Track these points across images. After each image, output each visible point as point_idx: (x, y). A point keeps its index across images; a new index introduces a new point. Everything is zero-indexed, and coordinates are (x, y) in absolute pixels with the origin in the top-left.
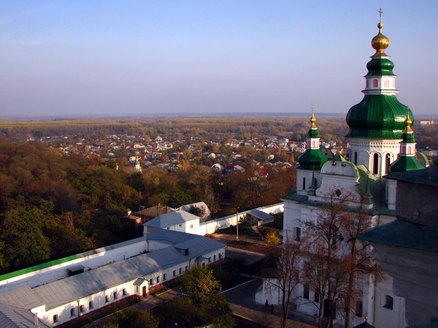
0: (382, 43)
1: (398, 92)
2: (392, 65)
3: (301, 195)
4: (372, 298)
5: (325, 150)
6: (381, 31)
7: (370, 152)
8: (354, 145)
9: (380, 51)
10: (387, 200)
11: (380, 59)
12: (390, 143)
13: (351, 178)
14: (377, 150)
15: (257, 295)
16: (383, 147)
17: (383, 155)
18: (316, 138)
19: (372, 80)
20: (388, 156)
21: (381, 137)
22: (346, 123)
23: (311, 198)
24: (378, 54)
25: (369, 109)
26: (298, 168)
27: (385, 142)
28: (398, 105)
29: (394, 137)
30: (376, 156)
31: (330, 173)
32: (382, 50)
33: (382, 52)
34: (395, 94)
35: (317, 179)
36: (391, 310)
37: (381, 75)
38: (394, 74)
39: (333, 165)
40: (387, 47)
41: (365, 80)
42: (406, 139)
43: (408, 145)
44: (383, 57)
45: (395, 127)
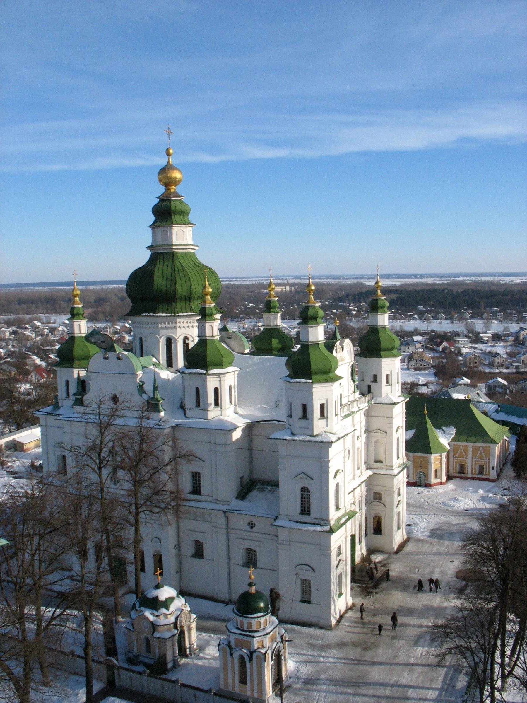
0: (172, 177)
6: (170, 160)
9: (170, 189)
14: (170, 333)
16: (178, 329)
17: (179, 340)
19: (159, 231)
30: (169, 342)
32: (173, 187)
33: (172, 190)
36: (201, 560)
39: (105, 358)
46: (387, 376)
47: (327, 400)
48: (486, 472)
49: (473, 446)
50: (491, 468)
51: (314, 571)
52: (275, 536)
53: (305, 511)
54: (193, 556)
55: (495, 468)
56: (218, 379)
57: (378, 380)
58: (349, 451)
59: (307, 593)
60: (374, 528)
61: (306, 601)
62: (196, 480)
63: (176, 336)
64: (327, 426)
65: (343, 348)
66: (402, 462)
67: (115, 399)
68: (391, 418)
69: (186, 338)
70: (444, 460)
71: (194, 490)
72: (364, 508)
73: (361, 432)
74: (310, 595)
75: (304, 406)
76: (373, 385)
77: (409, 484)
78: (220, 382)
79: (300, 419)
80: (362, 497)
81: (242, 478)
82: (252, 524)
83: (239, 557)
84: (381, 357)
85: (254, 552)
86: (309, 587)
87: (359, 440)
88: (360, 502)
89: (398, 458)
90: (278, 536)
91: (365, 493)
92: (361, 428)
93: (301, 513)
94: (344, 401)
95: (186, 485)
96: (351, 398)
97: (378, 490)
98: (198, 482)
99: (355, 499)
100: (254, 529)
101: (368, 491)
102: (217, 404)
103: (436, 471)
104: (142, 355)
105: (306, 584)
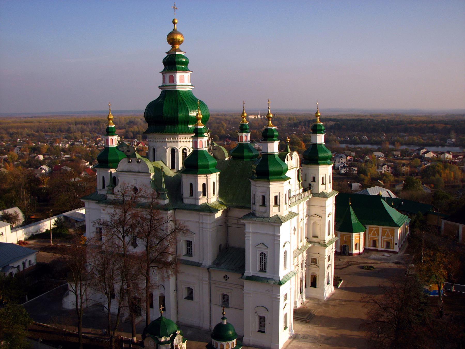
1: (193, 87)
2: (187, 61)
3: (101, 195)
4: (174, 291)
5: (127, 147)
6: (176, 27)
7: (167, 147)
8: (152, 141)
9: (175, 47)
10: (183, 195)
11: (175, 55)
12: (186, 138)
13: (146, 174)
14: (173, 145)
15: (65, 300)
16: (179, 143)
17: (180, 150)
18: (114, 135)
21: (177, 133)
22: (145, 119)
23: (111, 197)
24: (174, 50)
25: (164, 105)
26: (97, 167)
27: (181, 138)
28: (193, 100)
29: (187, 132)
30: (173, 151)
31: (127, 171)
32: (178, 46)
33: (177, 48)
34: (191, 90)
35: (116, 177)
36: (192, 301)
37: (176, 70)
38: (190, 69)
39: (129, 162)
40: (182, 43)
41: (161, 75)
42: (198, 133)
43: (199, 140)
44: (177, 53)
45: (190, 121)
46: (323, 178)
47: (279, 193)
48: (391, 247)
49: (382, 228)
50: (395, 244)
51: (268, 311)
52: (242, 286)
53: (262, 269)
54: (186, 298)
55: (398, 244)
56: (206, 177)
57: (316, 180)
58: (295, 229)
59: (263, 326)
60: (311, 283)
61: (262, 331)
62: (189, 247)
64: (279, 211)
65: (292, 158)
67: (135, 190)
68: (325, 207)
69: (185, 149)
70: (362, 237)
71: (187, 253)
72: (305, 269)
73: (303, 216)
74: (265, 327)
75: (264, 197)
76: (313, 184)
77: (336, 253)
78: (207, 179)
79: (260, 206)
80: (303, 261)
81: (220, 245)
82: (227, 277)
83: (218, 299)
84: (319, 165)
85: (227, 297)
86: (265, 322)
87: (302, 222)
88: (302, 264)
89: (329, 234)
90: (244, 286)
91: (305, 259)
92: (303, 214)
93: (259, 271)
95: (183, 249)
96: (297, 192)
97: (315, 256)
98: (190, 248)
99: (298, 262)
100: (227, 281)
101: (308, 257)
102: (204, 194)
103: (356, 245)
104: (154, 161)
105: (262, 320)
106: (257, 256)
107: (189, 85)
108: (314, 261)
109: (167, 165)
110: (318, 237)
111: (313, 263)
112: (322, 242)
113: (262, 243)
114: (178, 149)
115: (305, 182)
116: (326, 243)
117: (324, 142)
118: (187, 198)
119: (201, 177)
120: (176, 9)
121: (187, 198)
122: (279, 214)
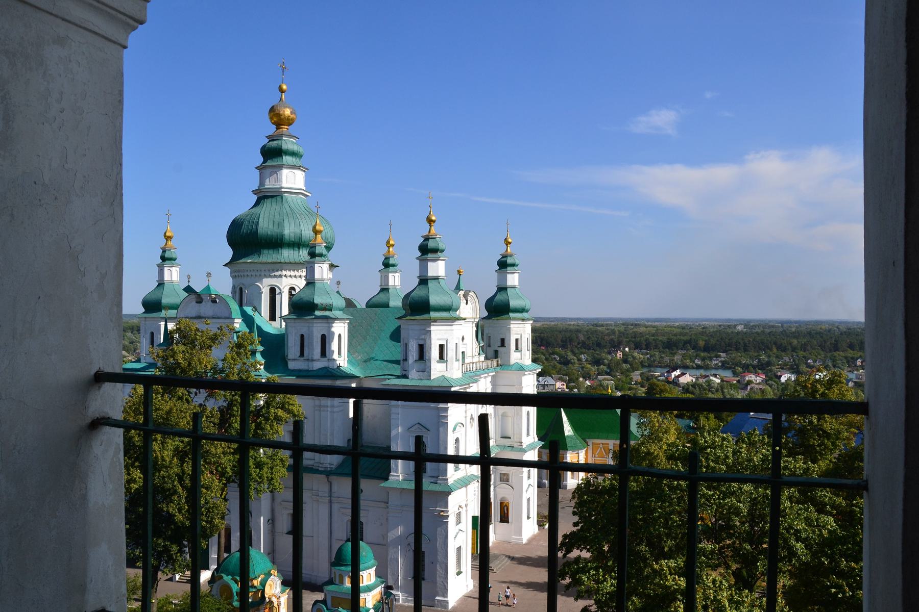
4: (269, 520)
10: (287, 356)
16: (283, 277)
20: (293, 291)
30: (273, 291)
39: (197, 302)
46: (517, 340)
49: (614, 444)
52: (385, 502)
63: (282, 285)
65: (467, 301)
66: (532, 441)
69: (292, 289)
76: (501, 350)
89: (528, 434)
94: (467, 360)
96: (476, 359)
106: (410, 447)
107: (303, 190)
108: (505, 477)
109: (262, 315)
110: (510, 438)
111: (503, 481)
112: (515, 445)
113: (419, 423)
114: (282, 288)
115: (488, 348)
116: (524, 447)
117: (518, 284)
118: (294, 360)
119: (319, 325)
120: (284, 69)
121: (294, 360)
122: (448, 375)
